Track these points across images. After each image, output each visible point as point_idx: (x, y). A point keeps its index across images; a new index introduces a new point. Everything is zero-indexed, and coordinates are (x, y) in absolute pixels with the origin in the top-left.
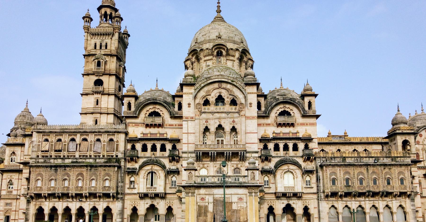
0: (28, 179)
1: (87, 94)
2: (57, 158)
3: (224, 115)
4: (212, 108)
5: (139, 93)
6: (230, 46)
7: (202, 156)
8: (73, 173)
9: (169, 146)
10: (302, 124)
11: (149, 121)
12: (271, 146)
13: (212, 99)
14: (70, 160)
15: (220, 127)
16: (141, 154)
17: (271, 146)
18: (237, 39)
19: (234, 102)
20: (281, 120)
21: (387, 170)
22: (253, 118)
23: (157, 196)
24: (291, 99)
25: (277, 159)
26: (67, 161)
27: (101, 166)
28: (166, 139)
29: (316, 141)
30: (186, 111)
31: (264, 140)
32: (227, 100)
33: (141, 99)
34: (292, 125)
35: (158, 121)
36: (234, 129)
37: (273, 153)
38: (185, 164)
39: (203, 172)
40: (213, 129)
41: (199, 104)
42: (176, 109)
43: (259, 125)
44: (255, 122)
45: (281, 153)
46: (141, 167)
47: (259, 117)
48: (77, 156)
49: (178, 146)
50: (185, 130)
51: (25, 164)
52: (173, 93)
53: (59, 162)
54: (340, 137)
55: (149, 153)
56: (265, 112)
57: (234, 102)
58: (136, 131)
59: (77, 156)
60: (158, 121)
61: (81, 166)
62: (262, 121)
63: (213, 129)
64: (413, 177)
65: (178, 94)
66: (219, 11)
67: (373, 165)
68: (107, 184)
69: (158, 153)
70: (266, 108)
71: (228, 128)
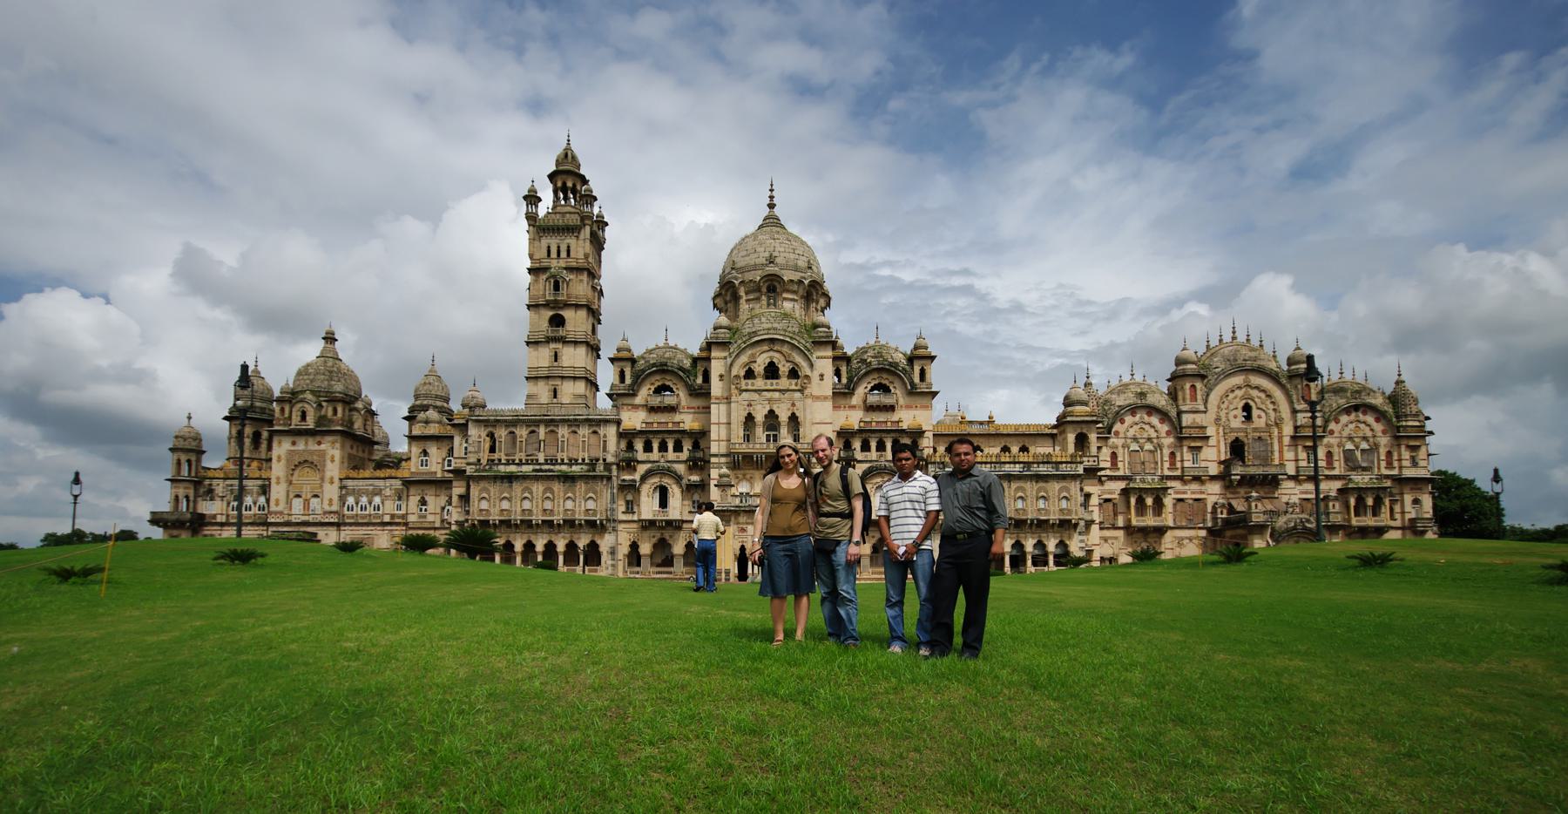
0: (465, 498)
1: (537, 343)
2: (508, 464)
3: (777, 395)
4: (760, 383)
5: (637, 353)
6: (787, 276)
7: (741, 463)
8: (538, 488)
9: (687, 446)
10: (908, 407)
11: (656, 401)
12: (857, 444)
13: (759, 368)
14: (531, 468)
15: (771, 414)
16: (641, 456)
17: (857, 444)
18: (802, 263)
19: (794, 374)
20: (875, 398)
21: (1041, 484)
22: (826, 398)
23: (669, 523)
24: (891, 364)
25: (866, 466)
26: (527, 469)
27: (581, 477)
28: (684, 432)
29: (929, 435)
30: (716, 388)
31: (846, 435)
32: (784, 368)
33: (641, 364)
34: (891, 408)
35: (669, 399)
36: (794, 419)
37: (859, 455)
38: (714, 473)
39: (743, 488)
40: (759, 417)
41: (737, 377)
42: (699, 380)
43: (835, 407)
44: (829, 404)
45: (873, 455)
46: (644, 478)
47: (837, 394)
48: (542, 460)
49: (702, 444)
50: (714, 419)
51: (459, 473)
52: (695, 352)
53: (513, 468)
54: (981, 423)
55: (655, 455)
56: (847, 386)
57: (794, 374)
58: (634, 419)
59: (542, 460)
60: (669, 399)
61: (548, 478)
62: (842, 402)
63: (759, 417)
64: (1088, 496)
65: (704, 354)
66: (771, 206)
67: (1019, 477)
68: (591, 505)
69: (671, 455)
70: (850, 379)
71: (784, 417)
